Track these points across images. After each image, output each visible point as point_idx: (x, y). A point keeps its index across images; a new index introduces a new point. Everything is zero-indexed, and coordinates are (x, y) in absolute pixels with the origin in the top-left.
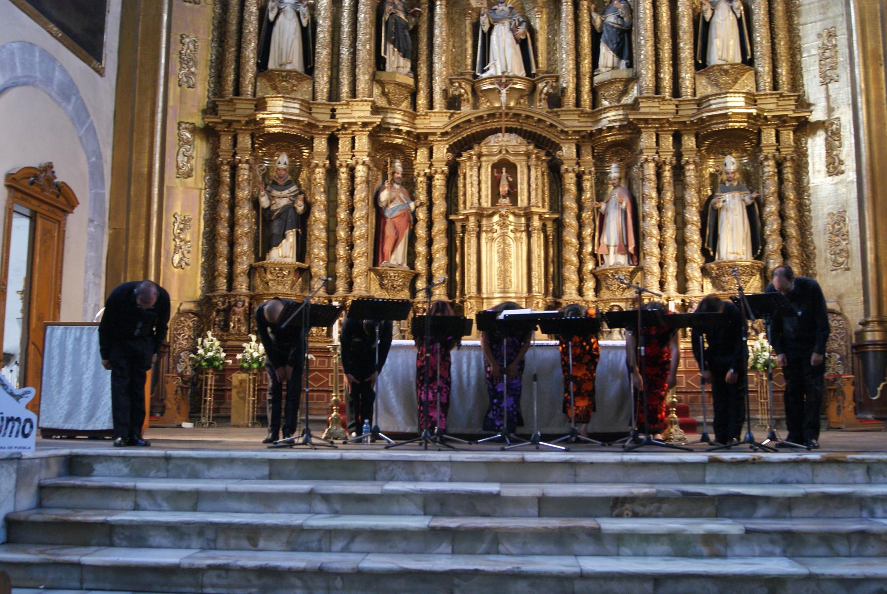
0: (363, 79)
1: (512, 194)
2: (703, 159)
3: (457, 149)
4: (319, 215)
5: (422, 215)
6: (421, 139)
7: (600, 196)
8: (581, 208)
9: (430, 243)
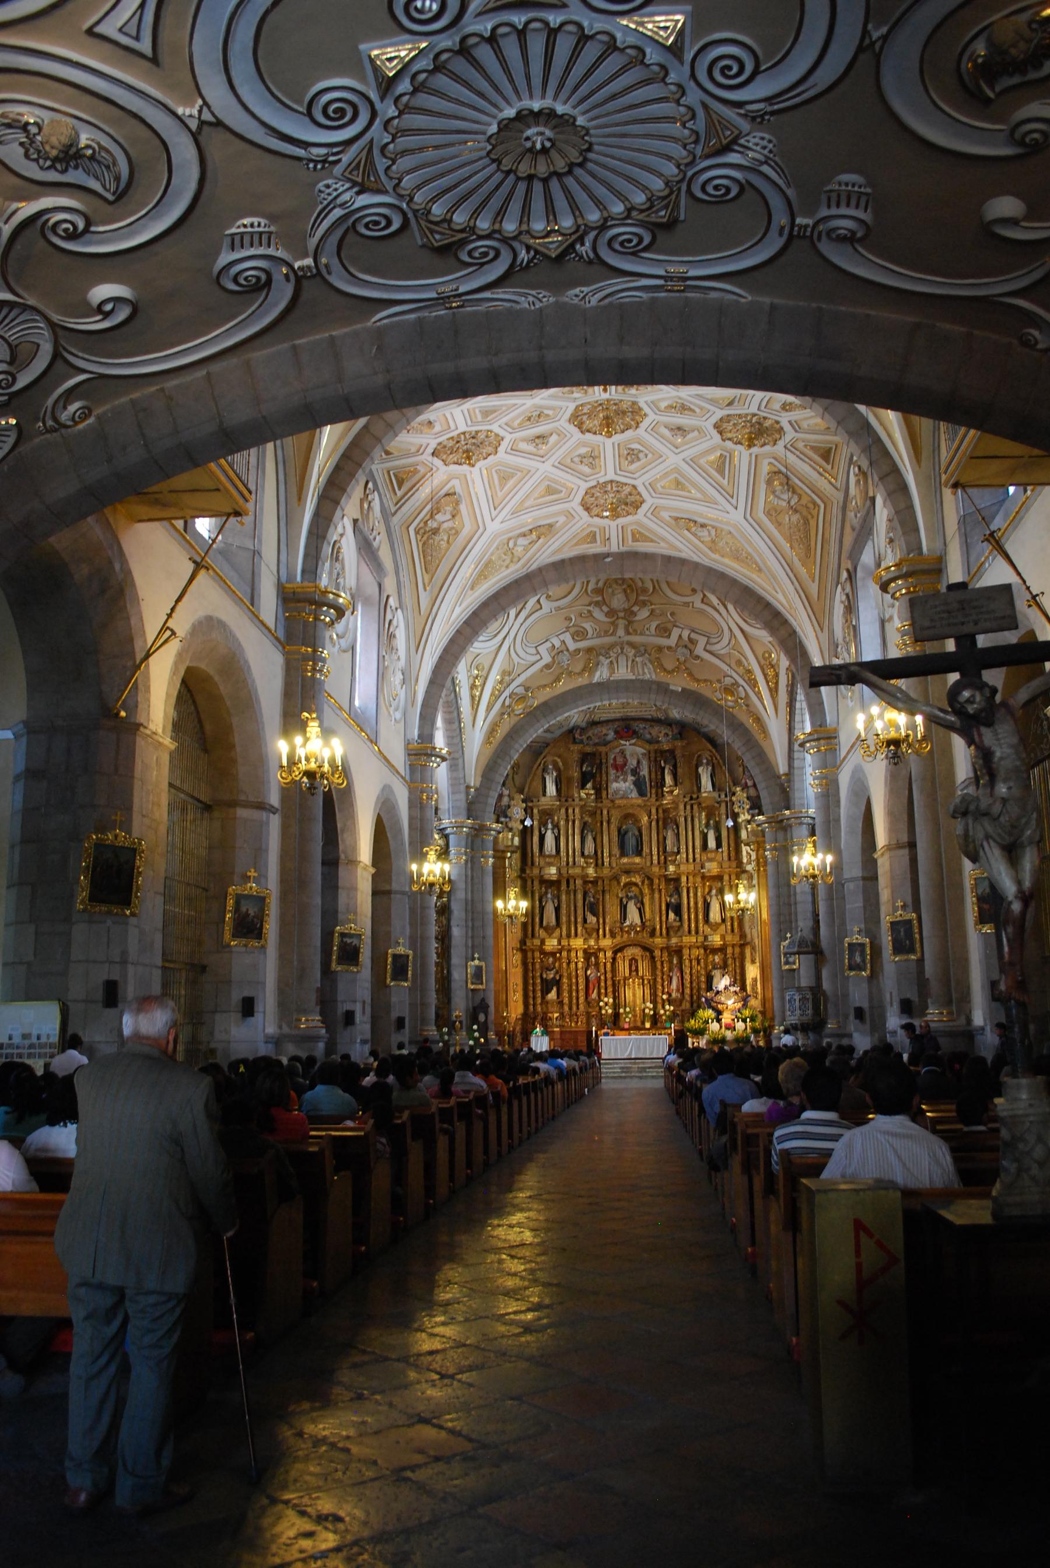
0: (580, 929)
1: (637, 970)
2: (707, 956)
3: (615, 953)
4: (565, 980)
5: (602, 978)
6: (600, 950)
7: (671, 970)
8: (663, 974)
9: (606, 989)
